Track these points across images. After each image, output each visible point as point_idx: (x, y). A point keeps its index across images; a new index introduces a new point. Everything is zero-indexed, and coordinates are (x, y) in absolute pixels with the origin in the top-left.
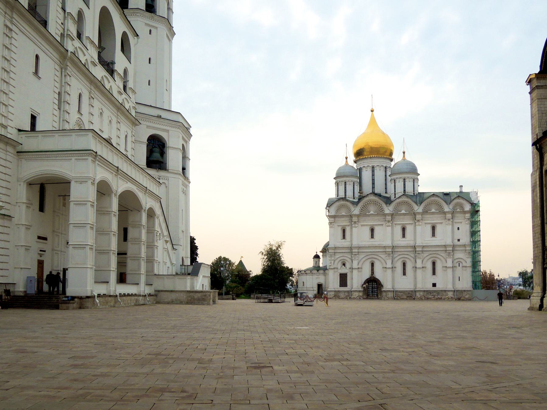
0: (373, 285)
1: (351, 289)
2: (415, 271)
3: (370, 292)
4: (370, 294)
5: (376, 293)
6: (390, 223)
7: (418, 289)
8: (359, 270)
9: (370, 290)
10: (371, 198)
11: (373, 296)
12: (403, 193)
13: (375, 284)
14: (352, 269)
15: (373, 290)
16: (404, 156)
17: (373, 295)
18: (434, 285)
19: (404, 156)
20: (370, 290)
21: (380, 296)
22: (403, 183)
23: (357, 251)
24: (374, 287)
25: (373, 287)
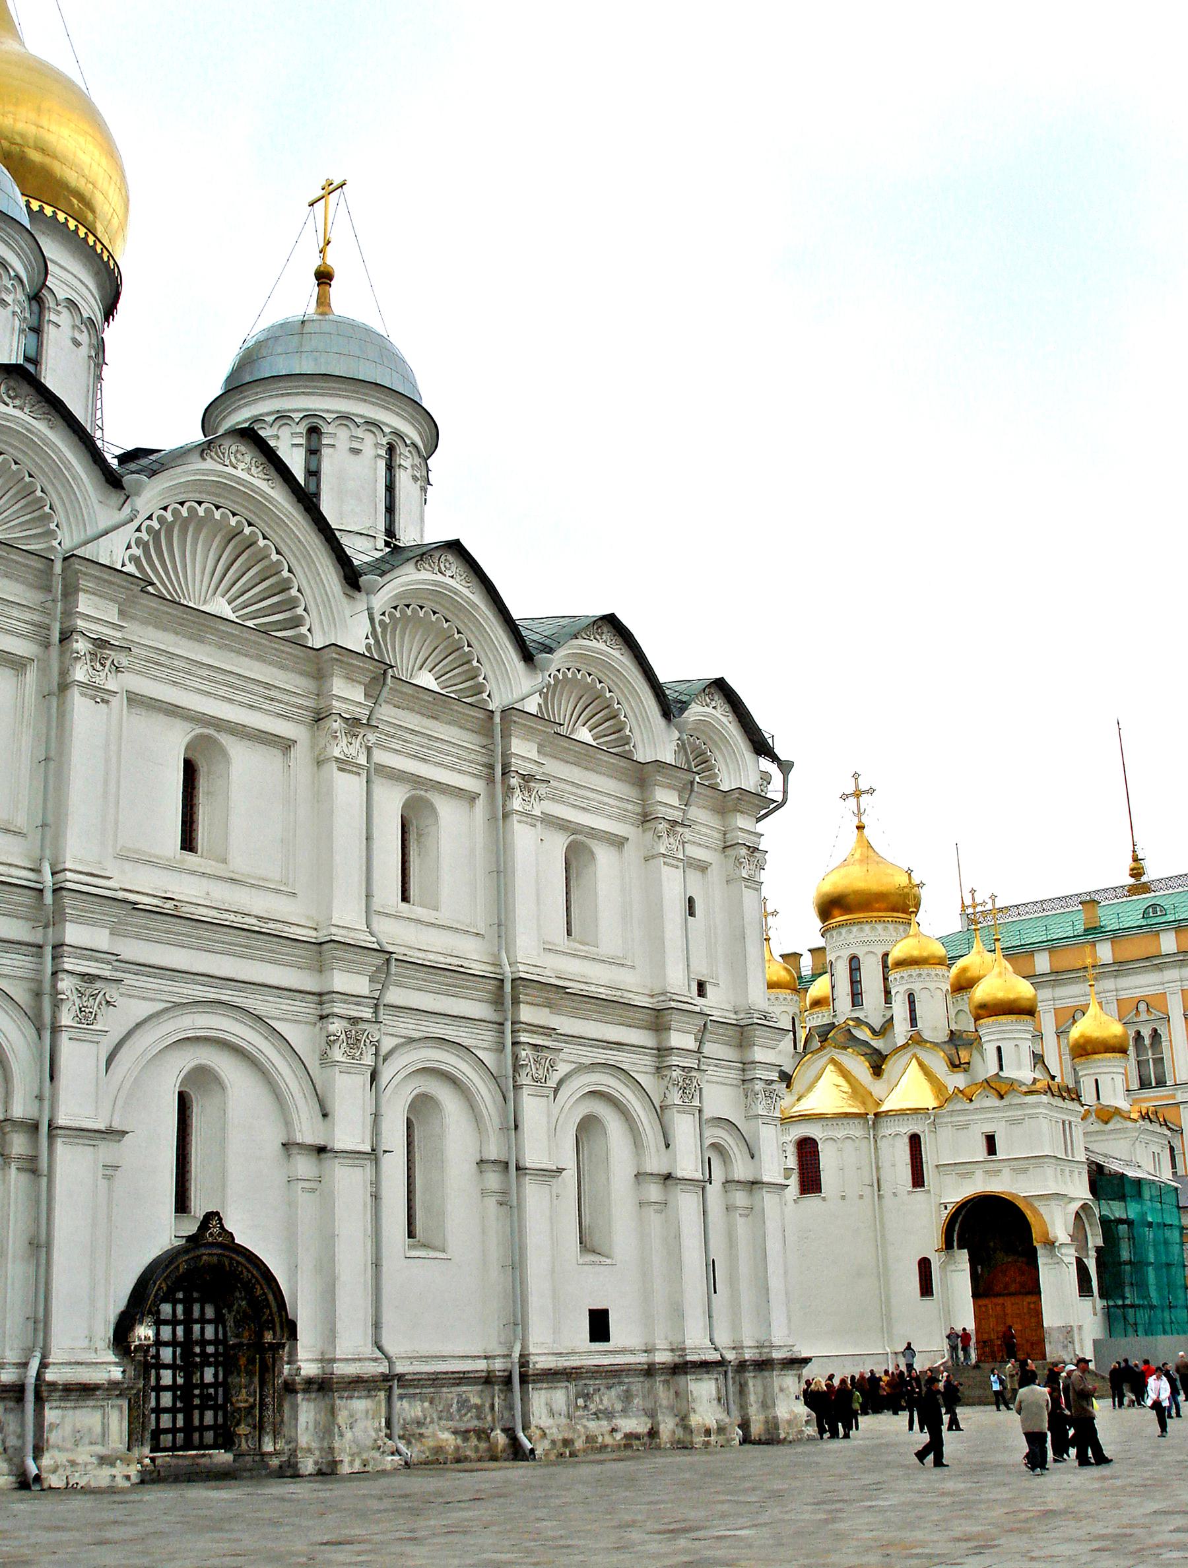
0: (188, 1323)
1: (39, 1376)
2: (509, 1202)
3: (167, 1399)
4: (166, 1421)
5: (215, 1408)
6: (357, 743)
7: (541, 1362)
8: (106, 1151)
9: (167, 1377)
10: (239, 473)
11: (188, 1446)
12: (380, 544)
13: (210, 1313)
14: (51, 1137)
15: (188, 1378)
16: (323, 302)
17: (188, 1428)
18: (599, 1325)
19: (323, 302)
20: (167, 1377)
21: (276, 1435)
22: (382, 464)
23: (99, 938)
24: (203, 1343)
25: (187, 1345)
